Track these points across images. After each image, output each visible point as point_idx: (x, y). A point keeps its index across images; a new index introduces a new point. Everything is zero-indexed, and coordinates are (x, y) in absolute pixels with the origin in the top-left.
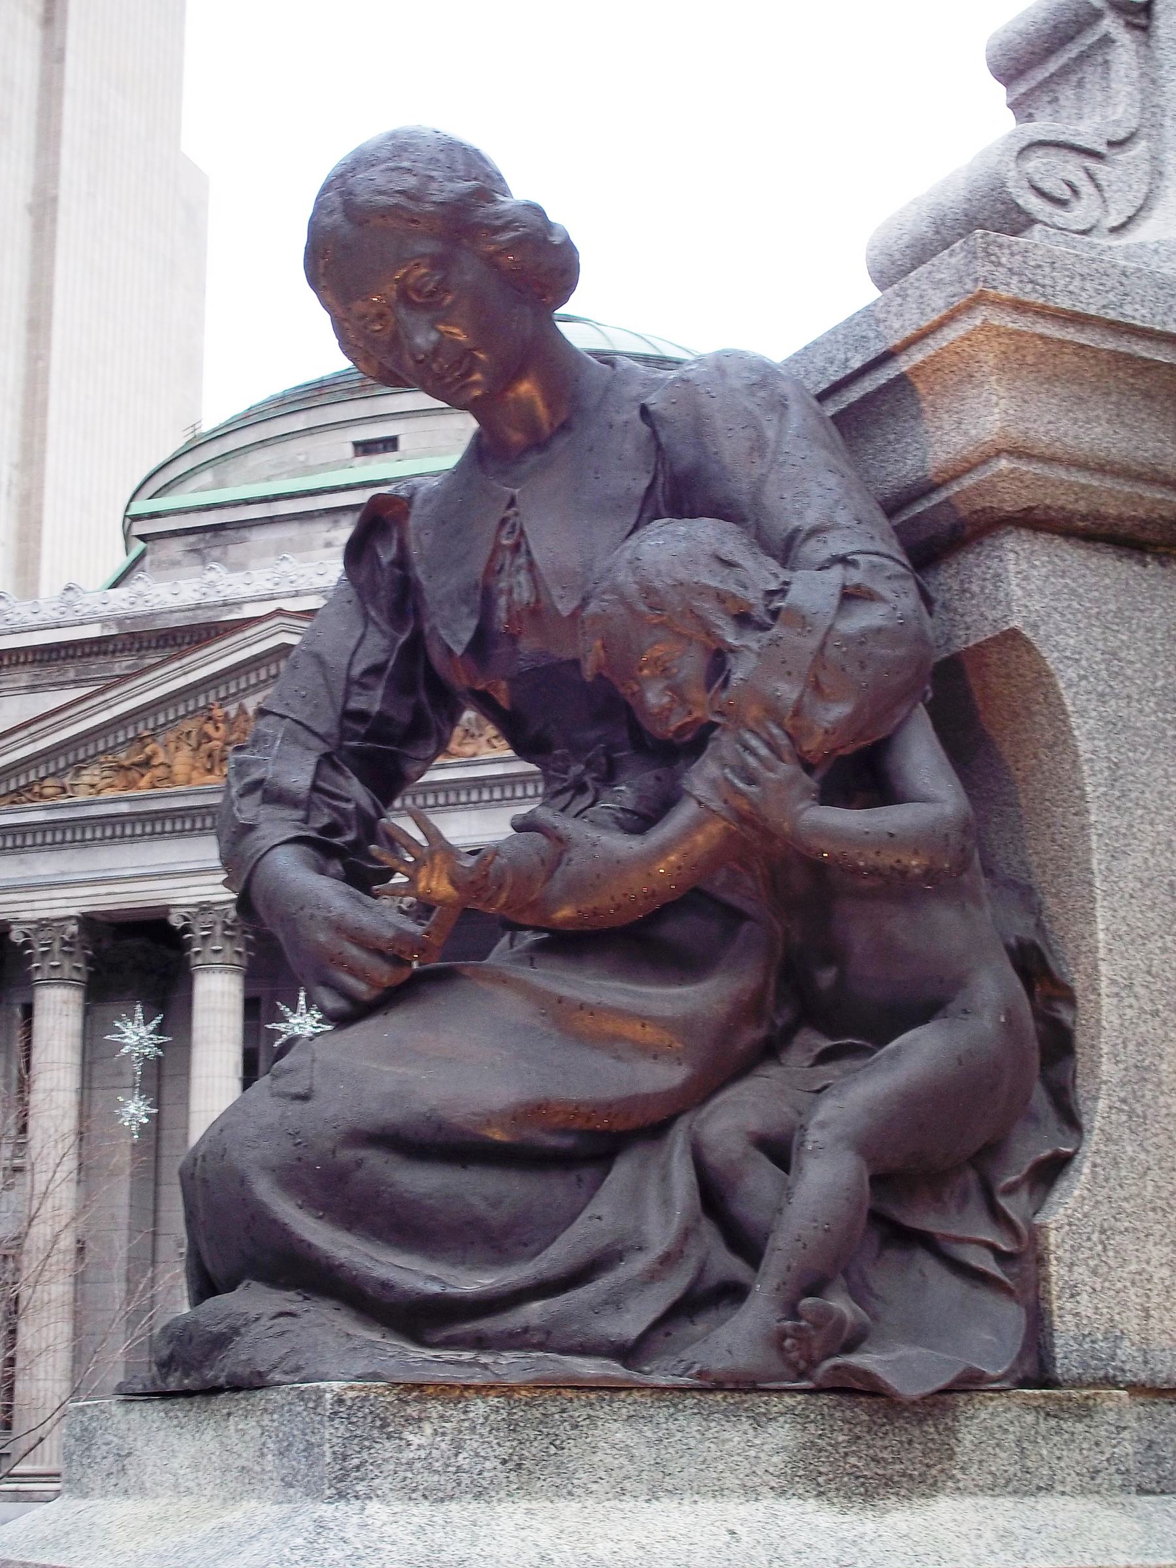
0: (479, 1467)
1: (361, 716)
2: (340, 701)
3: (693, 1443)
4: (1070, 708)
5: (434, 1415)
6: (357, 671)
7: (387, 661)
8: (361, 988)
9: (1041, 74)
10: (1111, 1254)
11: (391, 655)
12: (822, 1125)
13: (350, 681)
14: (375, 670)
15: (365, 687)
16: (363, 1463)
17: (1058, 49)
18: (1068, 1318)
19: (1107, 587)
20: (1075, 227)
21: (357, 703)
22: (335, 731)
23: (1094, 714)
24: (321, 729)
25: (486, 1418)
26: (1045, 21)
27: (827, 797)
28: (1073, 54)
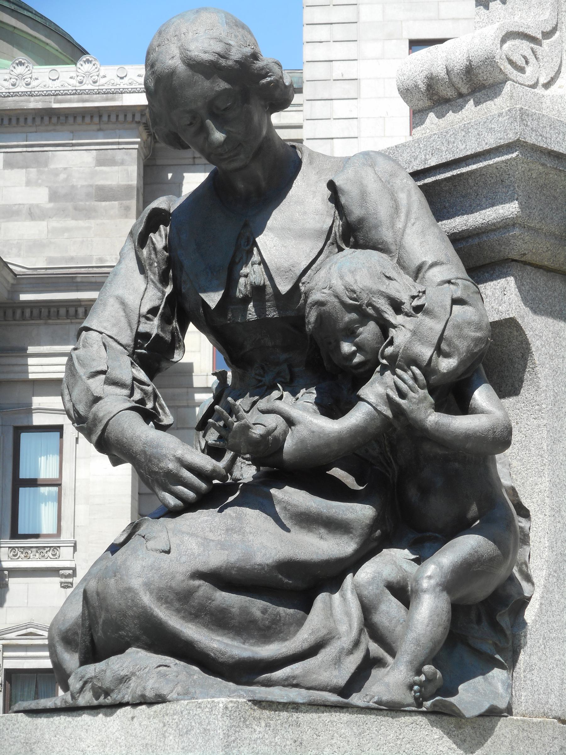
0: (284, 744)
1: (146, 336)
2: (135, 327)
3: (374, 736)
4: (537, 362)
5: (265, 716)
6: (144, 310)
7: (160, 305)
8: (191, 495)
10: (548, 650)
11: (162, 302)
12: (430, 577)
13: (140, 316)
14: (153, 311)
15: (148, 319)
16: (236, 739)
18: (528, 682)
19: (555, 297)
20: (527, 84)
21: (144, 327)
22: (132, 343)
23: (548, 366)
24: (124, 342)
25: (287, 719)
27: (438, 408)
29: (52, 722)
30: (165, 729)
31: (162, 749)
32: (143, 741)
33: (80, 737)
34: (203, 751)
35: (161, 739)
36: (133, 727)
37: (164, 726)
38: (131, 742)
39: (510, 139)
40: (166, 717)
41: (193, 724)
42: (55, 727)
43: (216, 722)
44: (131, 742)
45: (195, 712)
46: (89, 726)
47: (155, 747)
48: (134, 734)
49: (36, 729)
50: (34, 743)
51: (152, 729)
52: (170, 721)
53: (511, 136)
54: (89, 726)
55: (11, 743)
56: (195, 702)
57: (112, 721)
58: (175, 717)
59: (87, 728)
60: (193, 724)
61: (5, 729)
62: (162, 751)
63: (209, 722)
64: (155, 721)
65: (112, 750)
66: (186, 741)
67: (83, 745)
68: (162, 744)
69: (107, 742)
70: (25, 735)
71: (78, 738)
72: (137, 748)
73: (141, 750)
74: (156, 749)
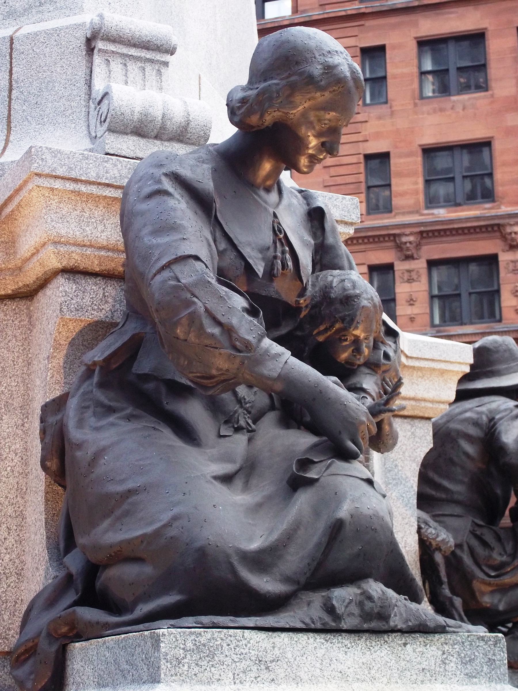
9: (124, 50)
17: (138, 48)
26: (146, 36)
28: (148, 56)
29: (296, 641)
30: (445, 656)
31: (442, 675)
32: (419, 666)
33: (337, 658)
34: (489, 678)
35: (441, 665)
36: (406, 653)
37: (444, 653)
38: (404, 666)
39: (353, 219)
40: (445, 646)
41: (477, 654)
42: (301, 646)
43: (502, 654)
44: (404, 666)
45: (478, 644)
46: (349, 648)
47: (434, 672)
48: (408, 659)
49: (274, 647)
50: (271, 662)
51: (429, 656)
52: (451, 650)
53: (354, 217)
54: (349, 648)
55: (236, 660)
56: (477, 635)
57: (379, 646)
58: (456, 646)
59: (346, 650)
60: (477, 654)
61: (225, 645)
62: (443, 676)
63: (494, 653)
64: (432, 648)
65: (380, 672)
66: (469, 668)
67: (341, 667)
68: (441, 670)
69: (374, 664)
70: (256, 653)
71: (334, 659)
72: (412, 672)
73: (416, 674)
74: (435, 674)
